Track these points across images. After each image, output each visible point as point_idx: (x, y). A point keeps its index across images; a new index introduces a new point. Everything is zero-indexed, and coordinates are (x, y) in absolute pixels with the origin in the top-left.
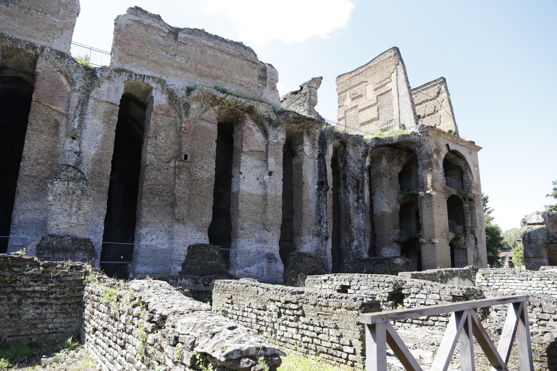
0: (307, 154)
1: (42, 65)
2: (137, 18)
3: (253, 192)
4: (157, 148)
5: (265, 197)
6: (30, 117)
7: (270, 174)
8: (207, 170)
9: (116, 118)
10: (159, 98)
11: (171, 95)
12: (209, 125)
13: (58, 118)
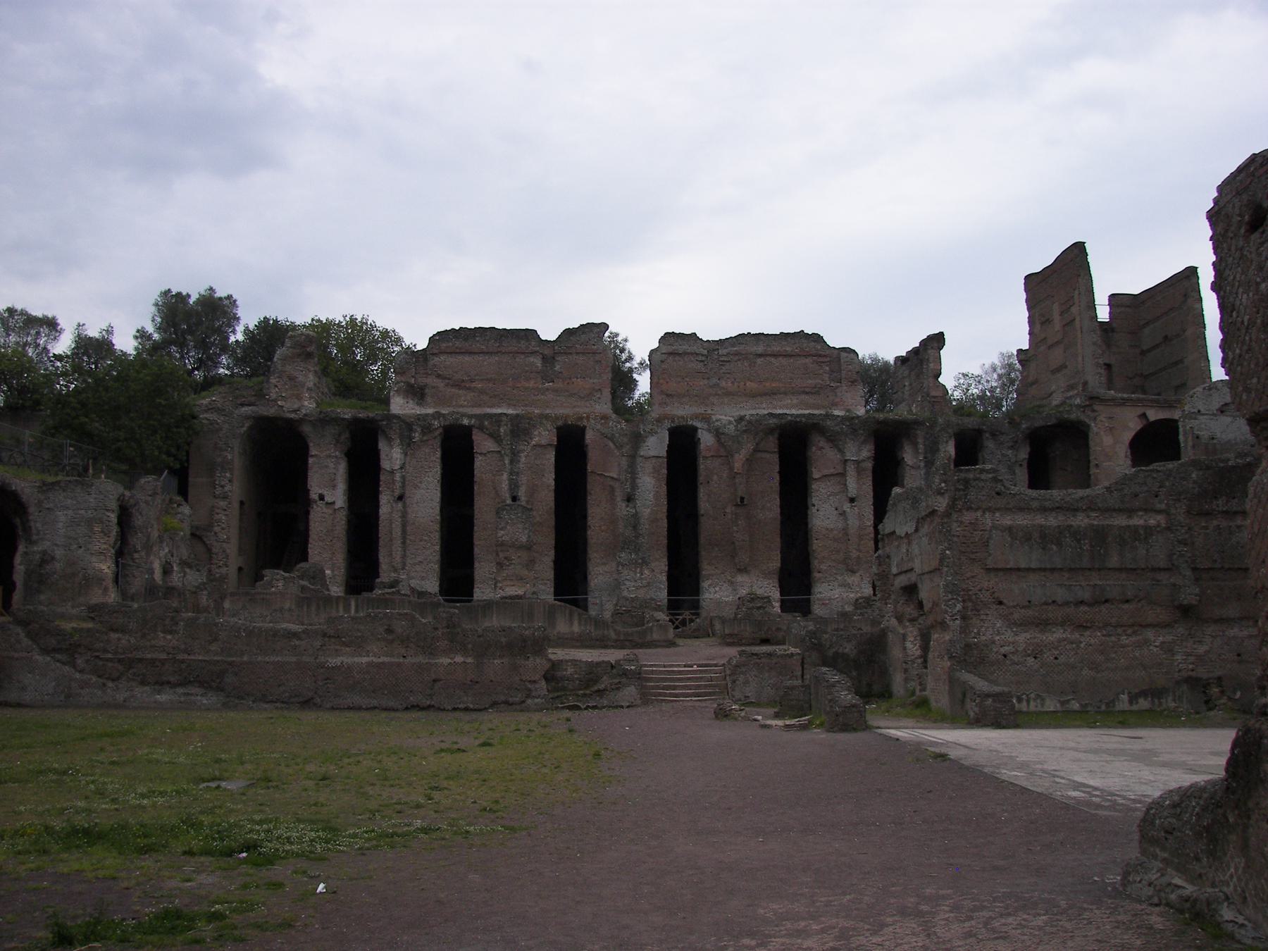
0: (910, 463)
1: (589, 436)
2: (670, 349)
3: (832, 526)
4: (712, 495)
5: (845, 531)
6: (589, 487)
7: (852, 500)
8: (770, 508)
9: (665, 471)
10: (706, 439)
11: (718, 433)
12: (768, 456)
13: (612, 483)
